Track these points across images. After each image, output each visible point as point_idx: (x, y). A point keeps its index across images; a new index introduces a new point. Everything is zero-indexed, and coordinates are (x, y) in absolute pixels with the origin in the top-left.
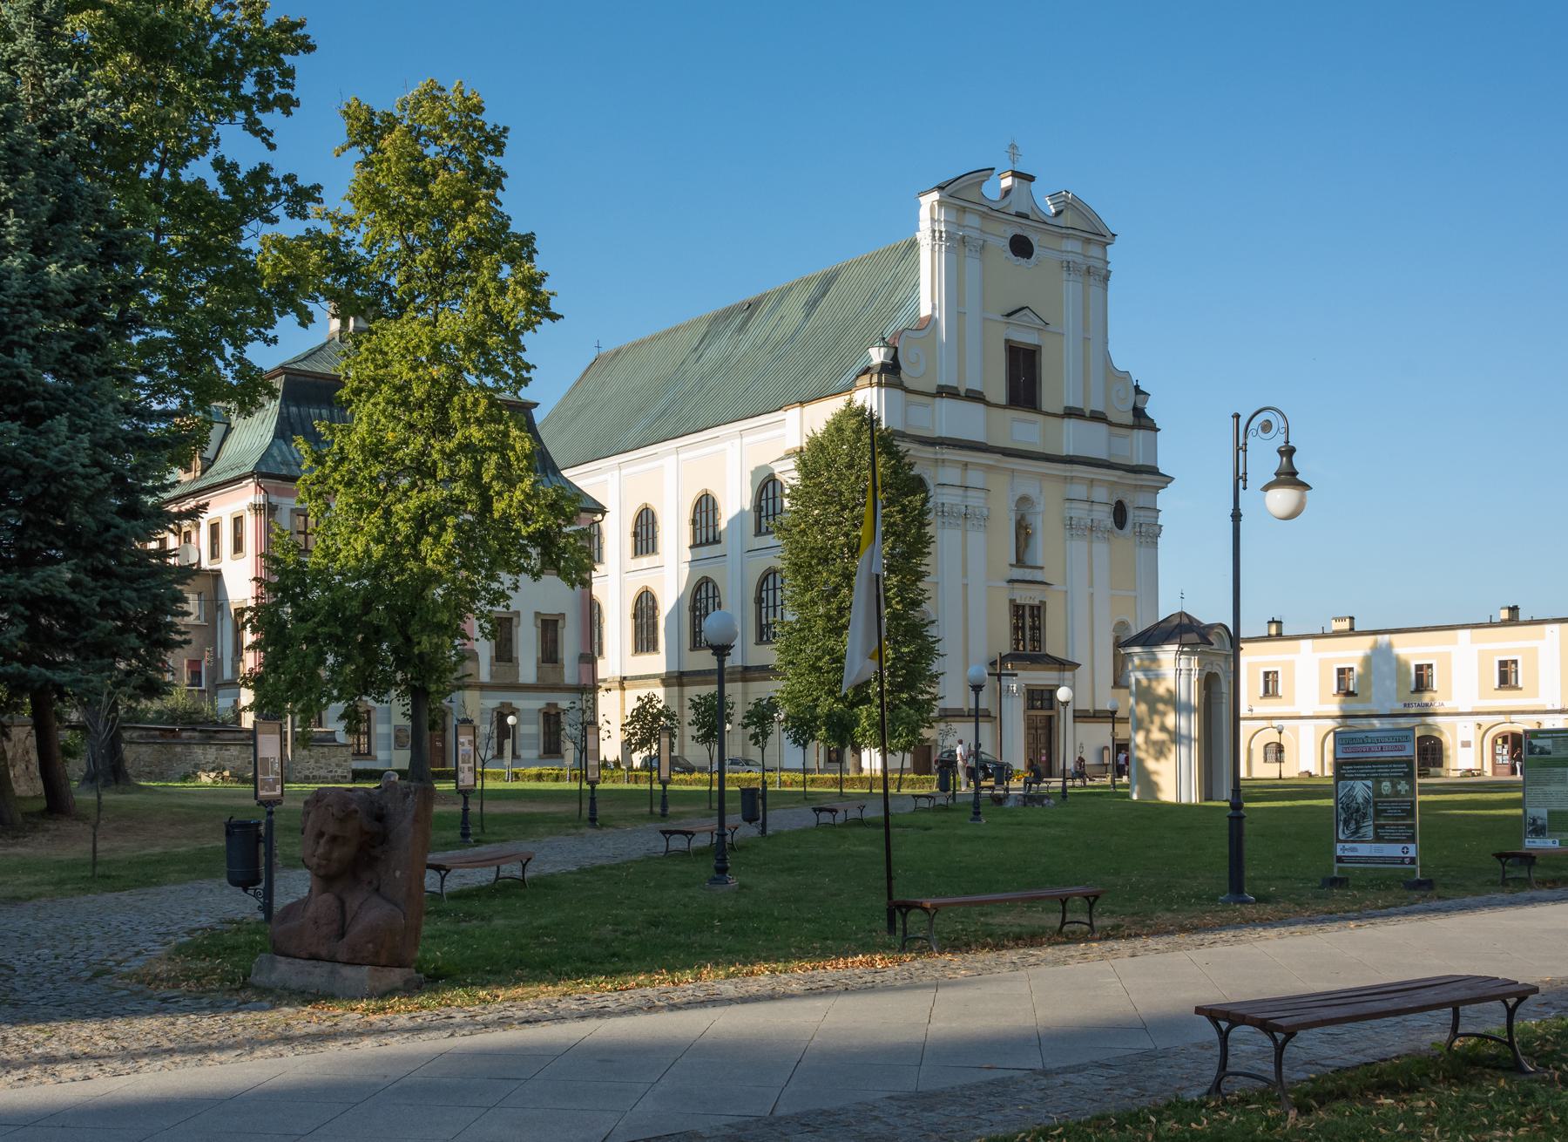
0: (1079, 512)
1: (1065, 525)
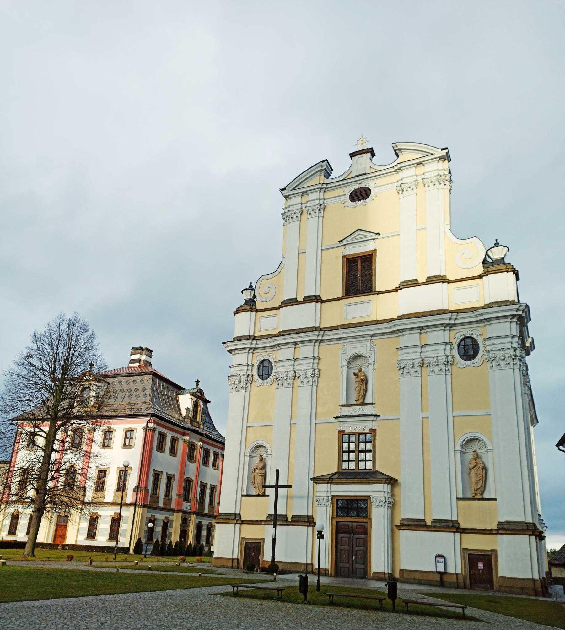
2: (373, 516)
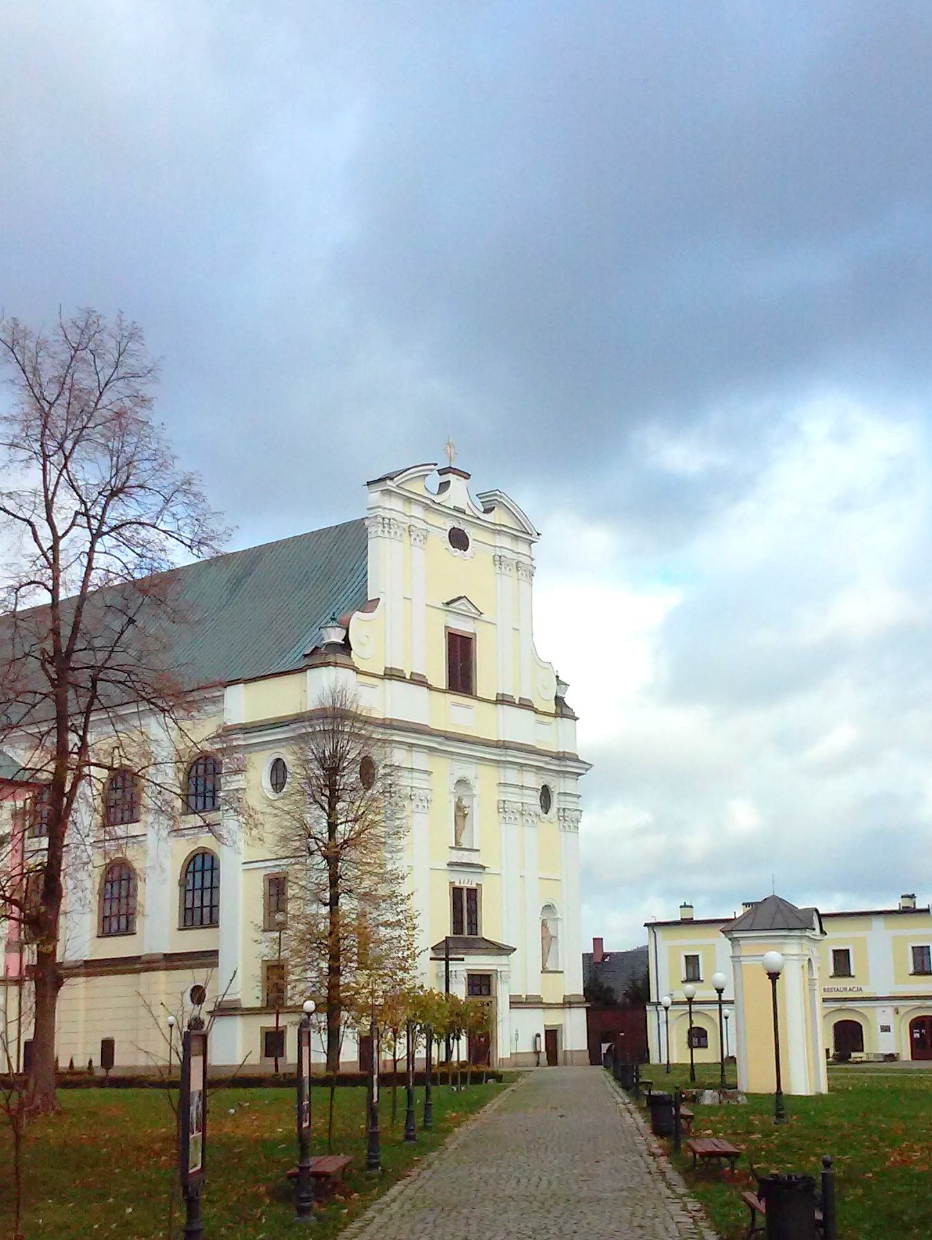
0: (513, 796)
1: (498, 808)
2: (499, 995)
